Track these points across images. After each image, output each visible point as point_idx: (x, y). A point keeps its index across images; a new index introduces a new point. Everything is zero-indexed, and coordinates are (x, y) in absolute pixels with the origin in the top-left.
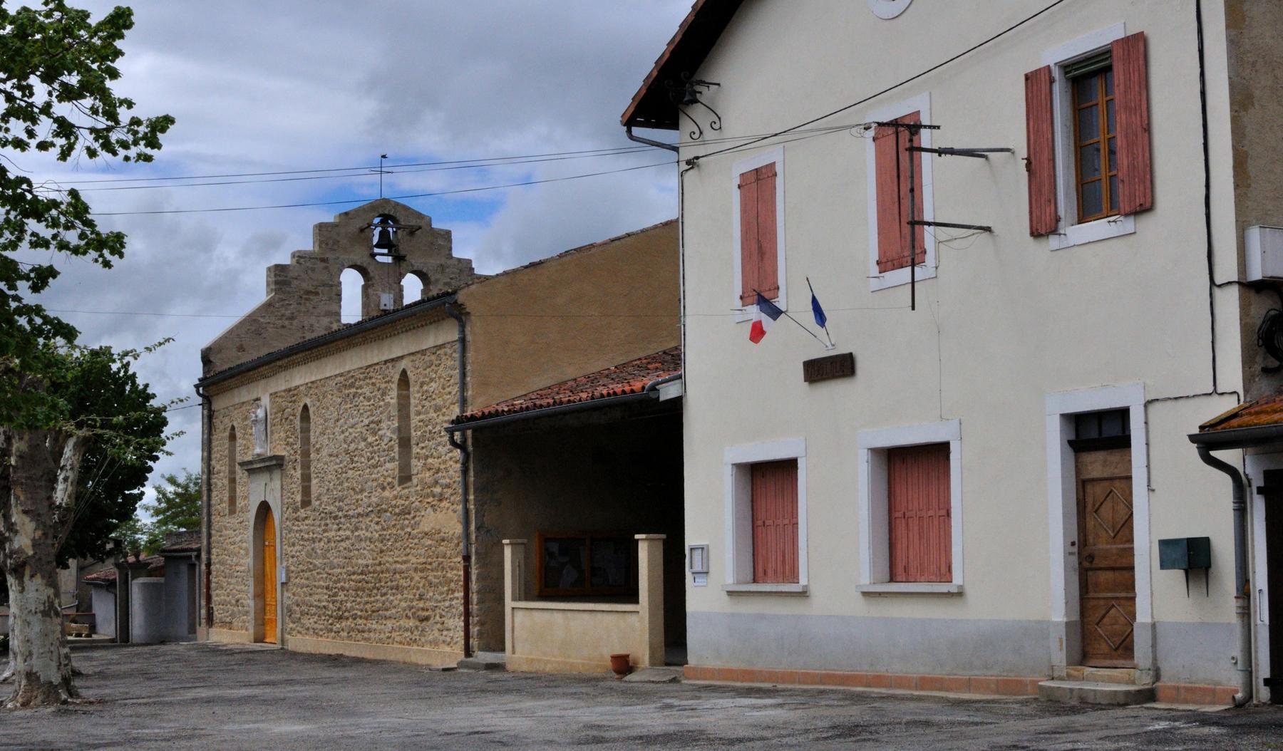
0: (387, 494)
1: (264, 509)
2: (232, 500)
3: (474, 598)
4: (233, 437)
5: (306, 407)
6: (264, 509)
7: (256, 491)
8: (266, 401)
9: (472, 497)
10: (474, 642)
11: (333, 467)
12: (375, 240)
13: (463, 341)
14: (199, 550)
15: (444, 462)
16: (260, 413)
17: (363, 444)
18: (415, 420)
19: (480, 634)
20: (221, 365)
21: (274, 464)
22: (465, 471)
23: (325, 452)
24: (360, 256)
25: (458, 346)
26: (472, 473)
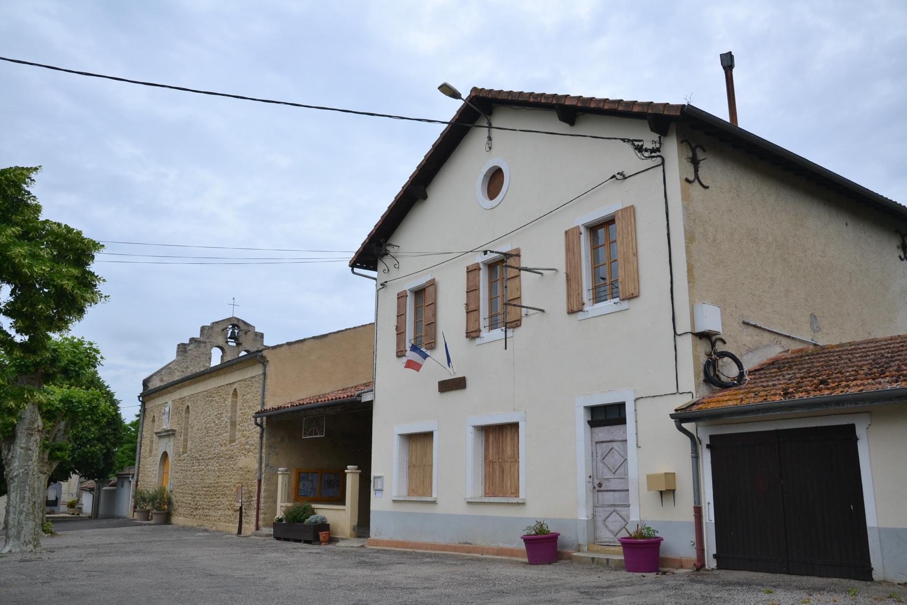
0: (223, 448)
1: (165, 455)
2: (151, 451)
3: (262, 500)
4: (153, 421)
5: (188, 407)
6: (165, 455)
7: (163, 446)
8: (170, 403)
9: (264, 450)
10: (260, 523)
11: (199, 435)
12: (229, 335)
13: (265, 374)
14: (133, 475)
15: (252, 432)
16: (167, 409)
17: (213, 425)
18: (239, 413)
19: (264, 519)
21: (170, 434)
22: (261, 438)
23: (195, 428)
24: (221, 341)
25: (262, 377)
26: (264, 439)
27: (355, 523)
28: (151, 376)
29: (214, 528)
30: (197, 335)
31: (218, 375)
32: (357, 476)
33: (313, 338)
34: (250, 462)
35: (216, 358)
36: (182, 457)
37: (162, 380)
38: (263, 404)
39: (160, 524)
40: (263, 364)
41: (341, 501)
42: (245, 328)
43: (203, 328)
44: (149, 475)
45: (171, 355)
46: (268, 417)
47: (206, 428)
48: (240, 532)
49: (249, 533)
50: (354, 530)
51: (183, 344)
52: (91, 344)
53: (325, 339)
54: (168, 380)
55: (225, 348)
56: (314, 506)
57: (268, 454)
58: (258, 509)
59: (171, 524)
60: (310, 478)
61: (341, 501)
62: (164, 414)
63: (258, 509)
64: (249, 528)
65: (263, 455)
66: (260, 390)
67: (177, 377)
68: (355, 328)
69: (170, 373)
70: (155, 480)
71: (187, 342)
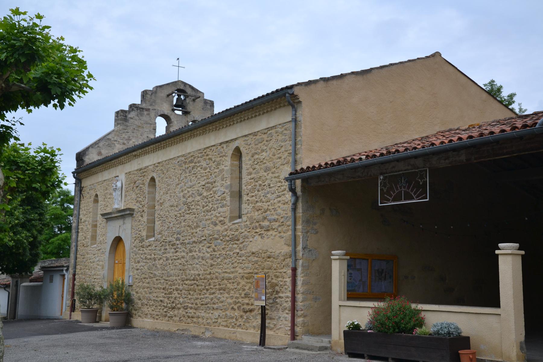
0: (218, 228)
1: (118, 240)
2: (94, 237)
3: (299, 297)
4: (96, 201)
5: (153, 179)
6: (118, 240)
7: (114, 229)
8: (122, 177)
9: (299, 227)
10: (298, 329)
11: (172, 214)
12: (175, 103)
13: (295, 120)
14: (68, 267)
15: (280, 201)
16: (119, 184)
17: (198, 198)
18: (245, 178)
19: (304, 324)
20: (92, 158)
21: (125, 214)
22: (294, 209)
23: (167, 204)
24: (166, 109)
25: (292, 125)
26: (300, 210)
27: (522, 338)
28: (87, 149)
29: (208, 334)
30: (138, 101)
31: (204, 133)
32: (519, 260)
33: (353, 73)
34: (277, 244)
35: (161, 127)
36: (146, 243)
37: (100, 154)
38: (295, 162)
39: (121, 328)
40: (293, 107)
41: (492, 299)
42: (193, 93)
43: (144, 94)
44: (93, 265)
45: (108, 125)
46: (305, 181)
47: (185, 203)
48: (262, 342)
49: (279, 343)
50: (521, 348)
51: (123, 111)
52: (75, 51)
53: (369, 76)
54: (107, 152)
55: (172, 117)
56: (420, 307)
57: (306, 232)
58: (293, 309)
59: (132, 327)
60: (358, 267)
61: (492, 299)
62: (115, 190)
63: (293, 309)
64: (279, 334)
65: (299, 233)
66: (288, 145)
67: (118, 148)
68: (401, 63)
69: (109, 146)
70: (105, 272)
71: (127, 109)
